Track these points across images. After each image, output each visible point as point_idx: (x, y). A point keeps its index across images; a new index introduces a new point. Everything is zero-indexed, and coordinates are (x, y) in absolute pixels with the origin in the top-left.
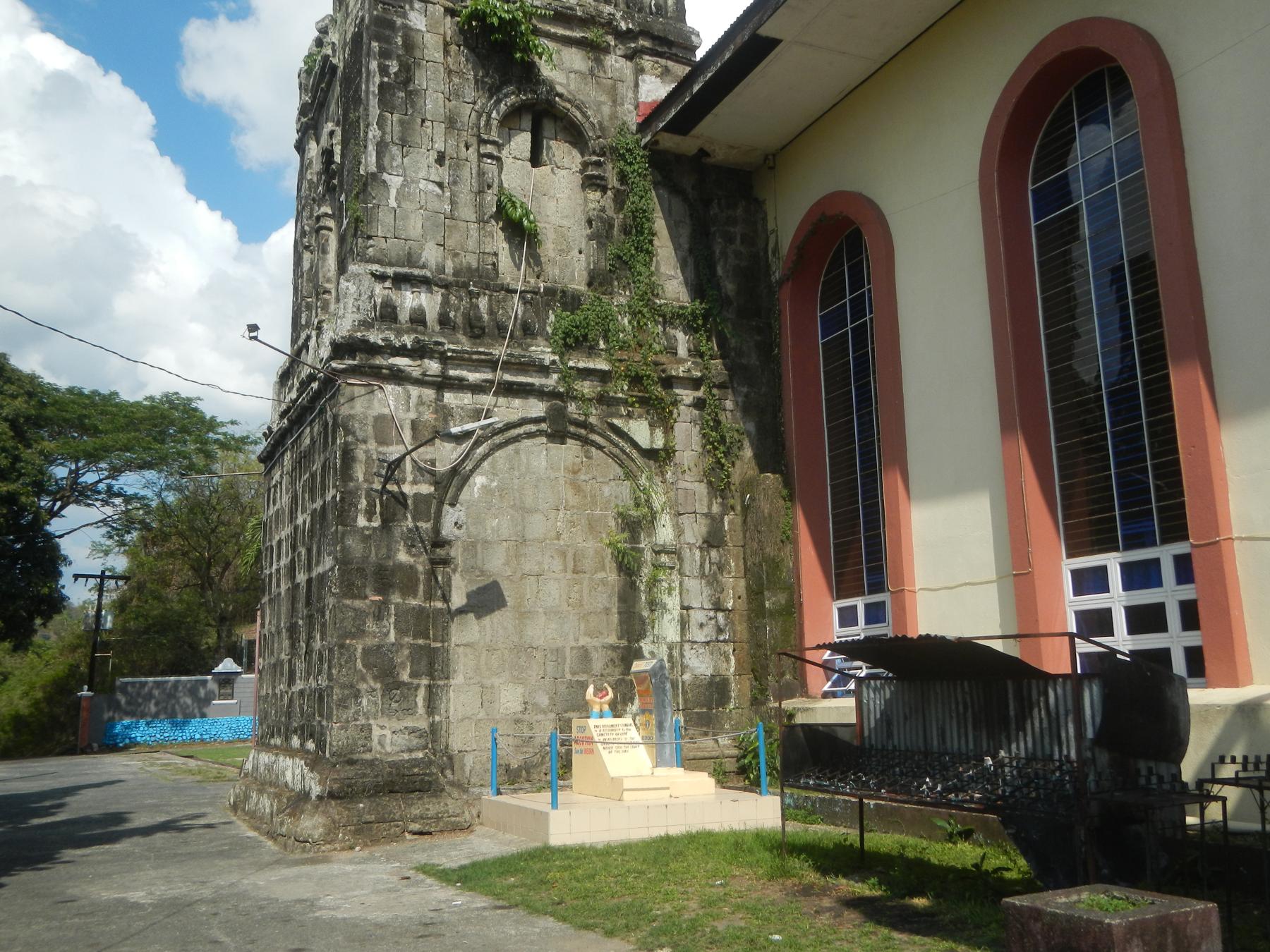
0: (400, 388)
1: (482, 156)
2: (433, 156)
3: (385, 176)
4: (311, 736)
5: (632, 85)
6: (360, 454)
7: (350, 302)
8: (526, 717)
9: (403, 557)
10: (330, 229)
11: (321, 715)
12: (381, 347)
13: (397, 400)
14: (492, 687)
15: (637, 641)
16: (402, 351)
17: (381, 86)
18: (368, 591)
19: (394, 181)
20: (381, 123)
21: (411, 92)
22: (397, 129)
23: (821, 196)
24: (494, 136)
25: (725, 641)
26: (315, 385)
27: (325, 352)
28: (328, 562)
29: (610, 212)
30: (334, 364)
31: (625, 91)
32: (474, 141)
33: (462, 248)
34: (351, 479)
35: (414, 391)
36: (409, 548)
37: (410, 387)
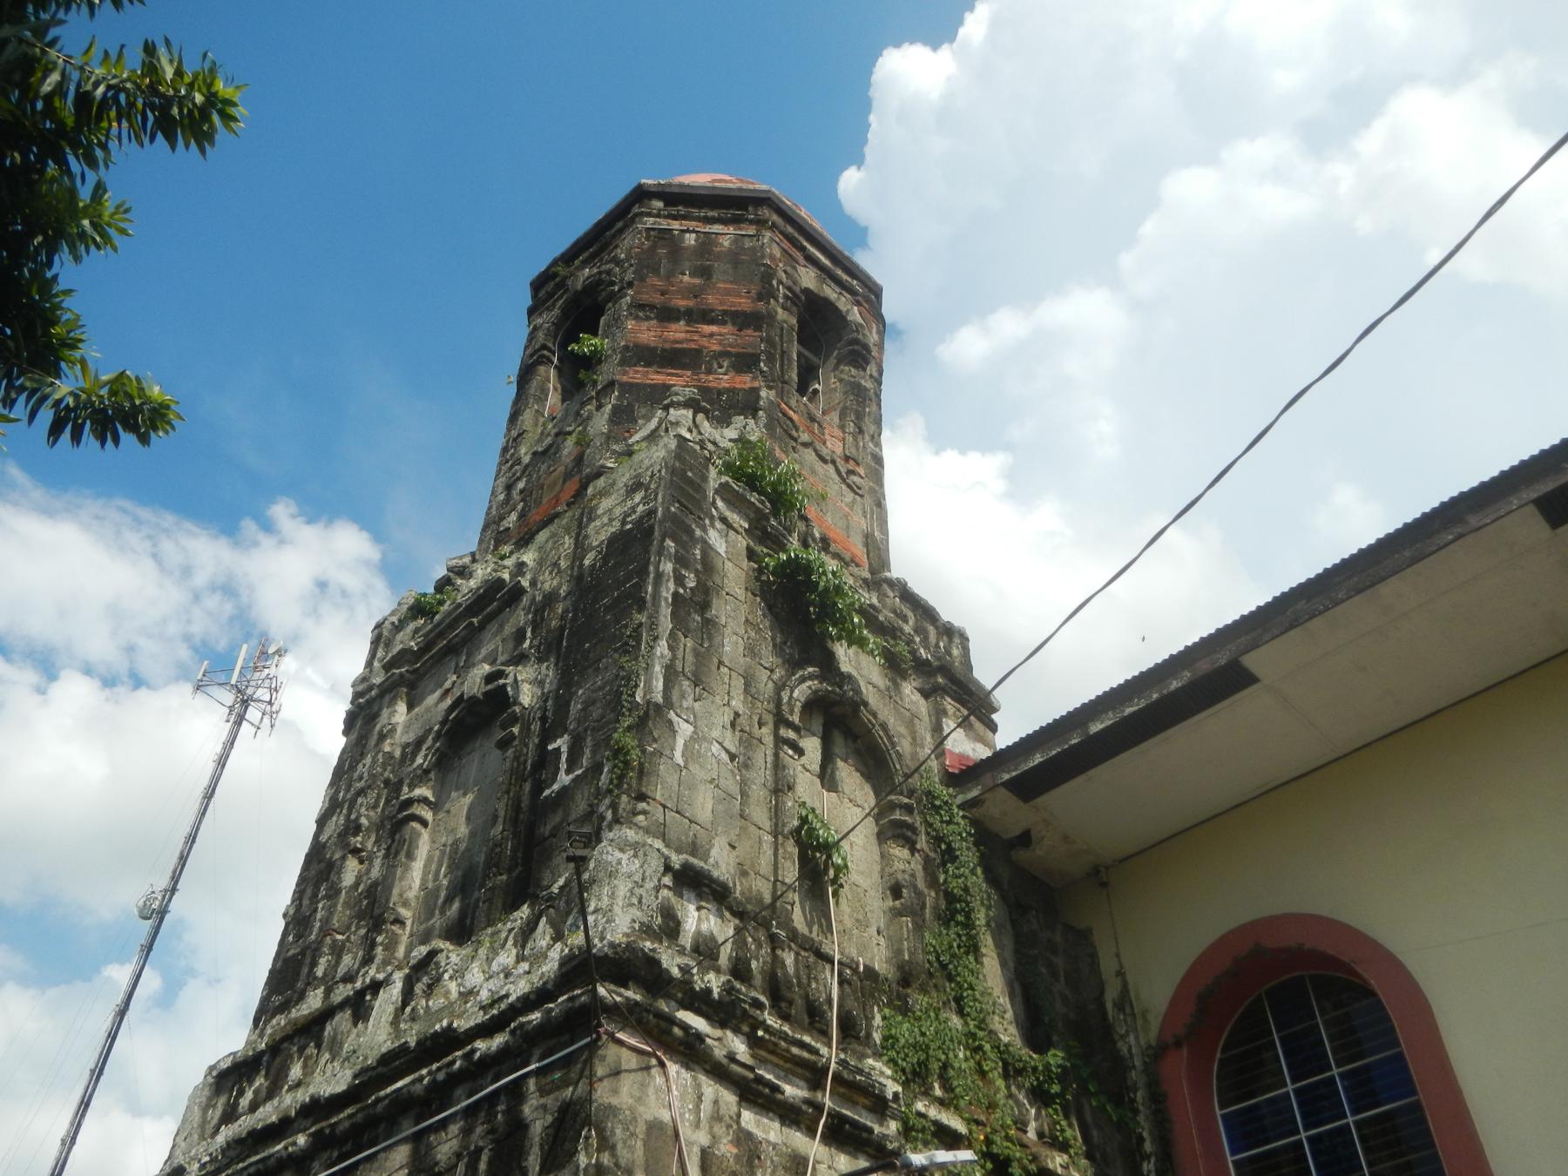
0: (686, 1075)
2: (727, 718)
3: (672, 715)
7: (623, 888)
10: (424, 823)
12: (671, 979)
13: (682, 1097)
16: (700, 1002)
17: (676, 595)
19: (685, 730)
22: (690, 658)
23: (1224, 931)
24: (796, 718)
32: (769, 719)
33: (752, 866)
35: (710, 1088)
37: (702, 1078)
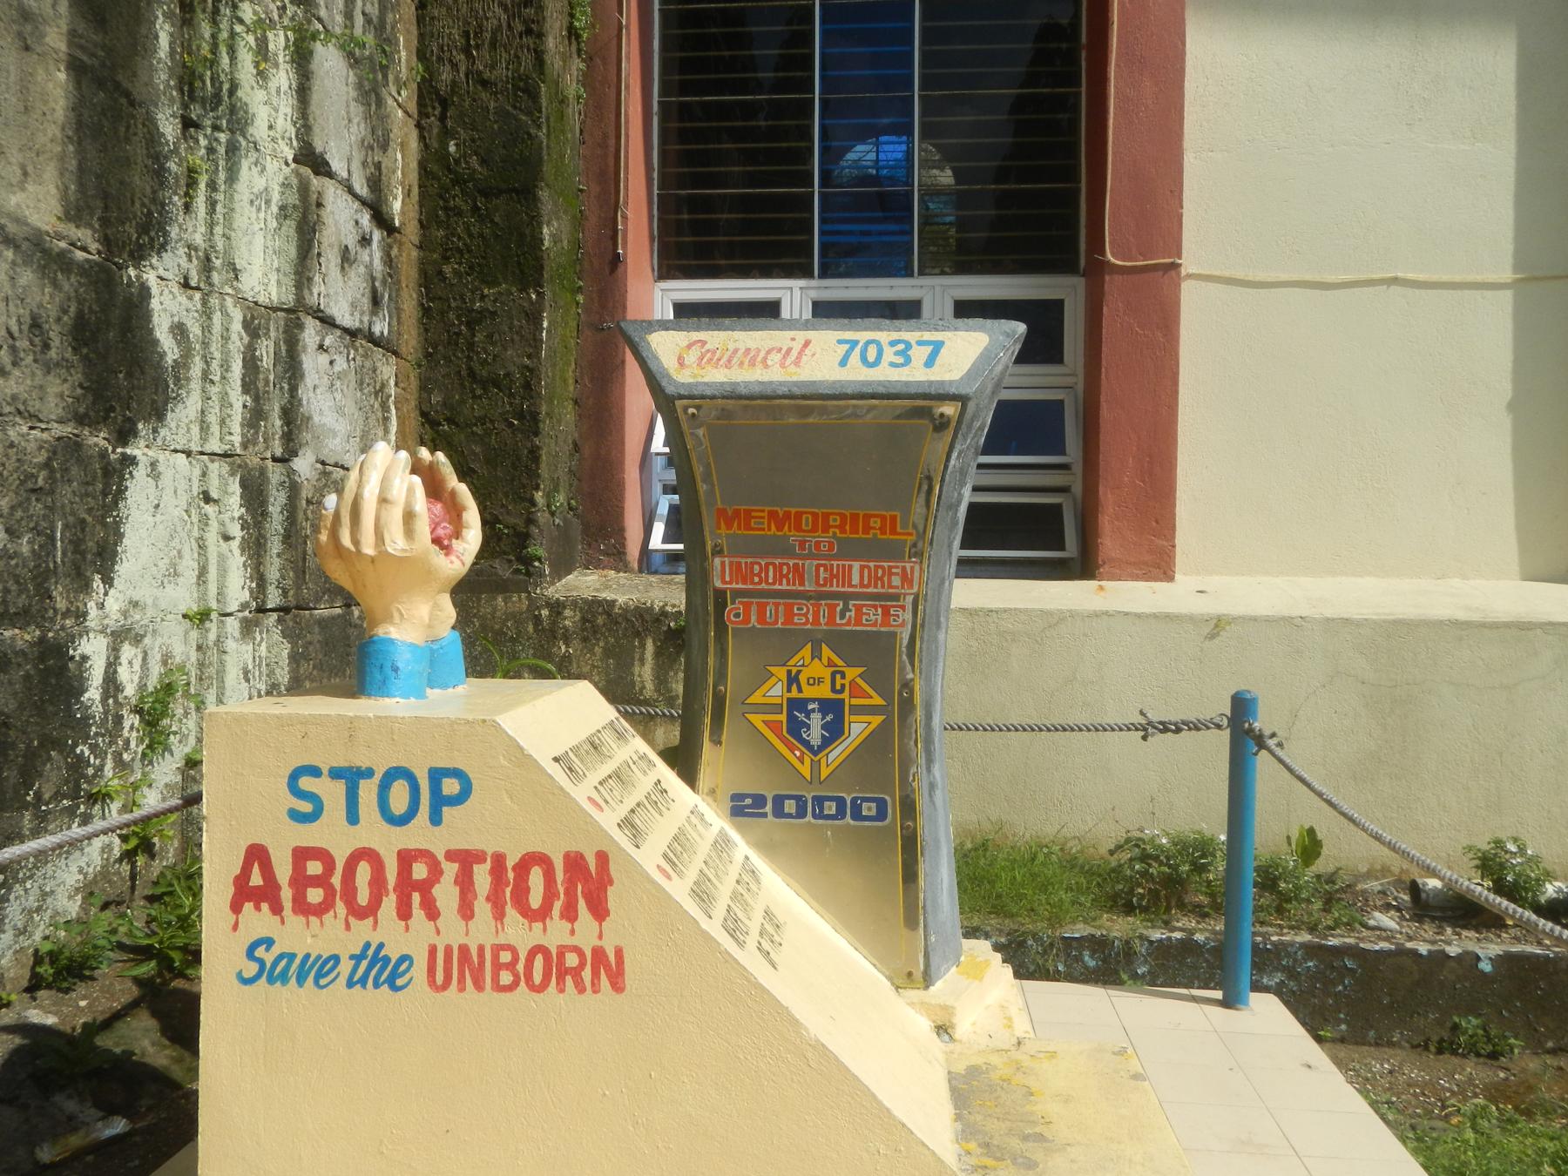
15: (138, 256)
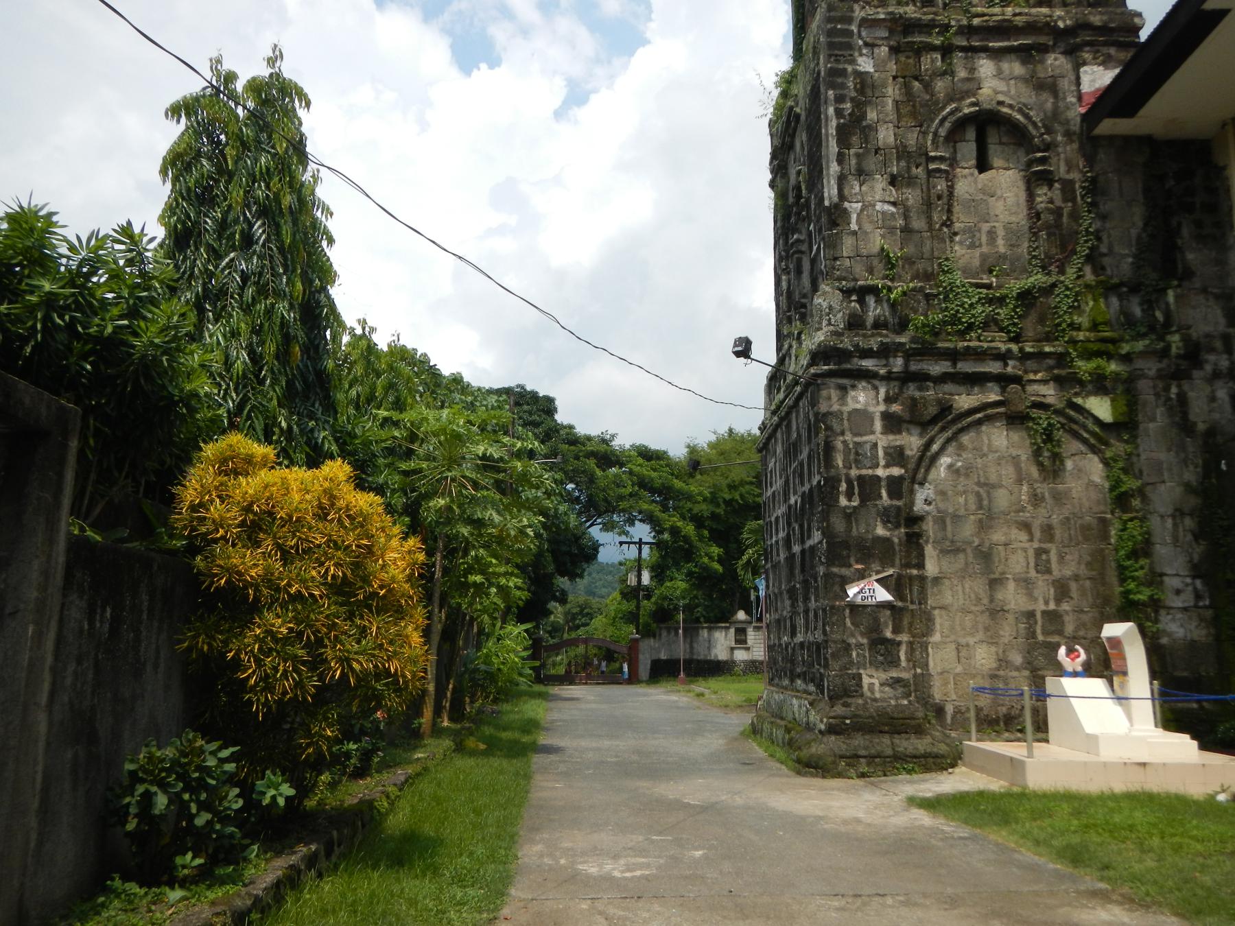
1: (930, 173)
3: (846, 204)
4: (812, 680)
5: (1073, 78)
6: (840, 446)
8: (1001, 673)
9: (880, 531)
11: (819, 664)
14: (968, 645)
16: (867, 354)
17: (839, 128)
18: (852, 560)
19: (854, 207)
20: (841, 159)
21: (865, 127)
25: (1205, 607)
26: (798, 389)
27: (804, 361)
28: (817, 536)
29: (1059, 203)
30: (812, 371)
31: (1065, 84)
34: (833, 467)
36: (885, 523)
